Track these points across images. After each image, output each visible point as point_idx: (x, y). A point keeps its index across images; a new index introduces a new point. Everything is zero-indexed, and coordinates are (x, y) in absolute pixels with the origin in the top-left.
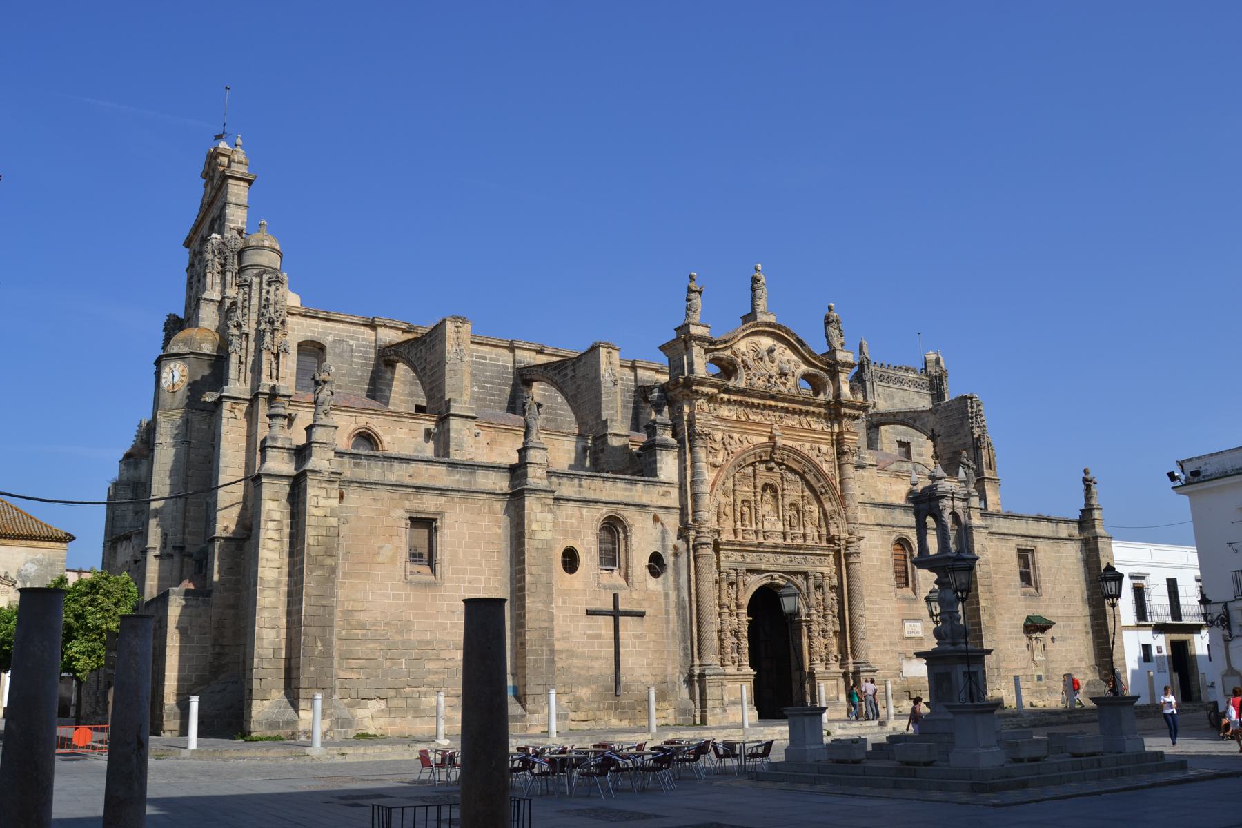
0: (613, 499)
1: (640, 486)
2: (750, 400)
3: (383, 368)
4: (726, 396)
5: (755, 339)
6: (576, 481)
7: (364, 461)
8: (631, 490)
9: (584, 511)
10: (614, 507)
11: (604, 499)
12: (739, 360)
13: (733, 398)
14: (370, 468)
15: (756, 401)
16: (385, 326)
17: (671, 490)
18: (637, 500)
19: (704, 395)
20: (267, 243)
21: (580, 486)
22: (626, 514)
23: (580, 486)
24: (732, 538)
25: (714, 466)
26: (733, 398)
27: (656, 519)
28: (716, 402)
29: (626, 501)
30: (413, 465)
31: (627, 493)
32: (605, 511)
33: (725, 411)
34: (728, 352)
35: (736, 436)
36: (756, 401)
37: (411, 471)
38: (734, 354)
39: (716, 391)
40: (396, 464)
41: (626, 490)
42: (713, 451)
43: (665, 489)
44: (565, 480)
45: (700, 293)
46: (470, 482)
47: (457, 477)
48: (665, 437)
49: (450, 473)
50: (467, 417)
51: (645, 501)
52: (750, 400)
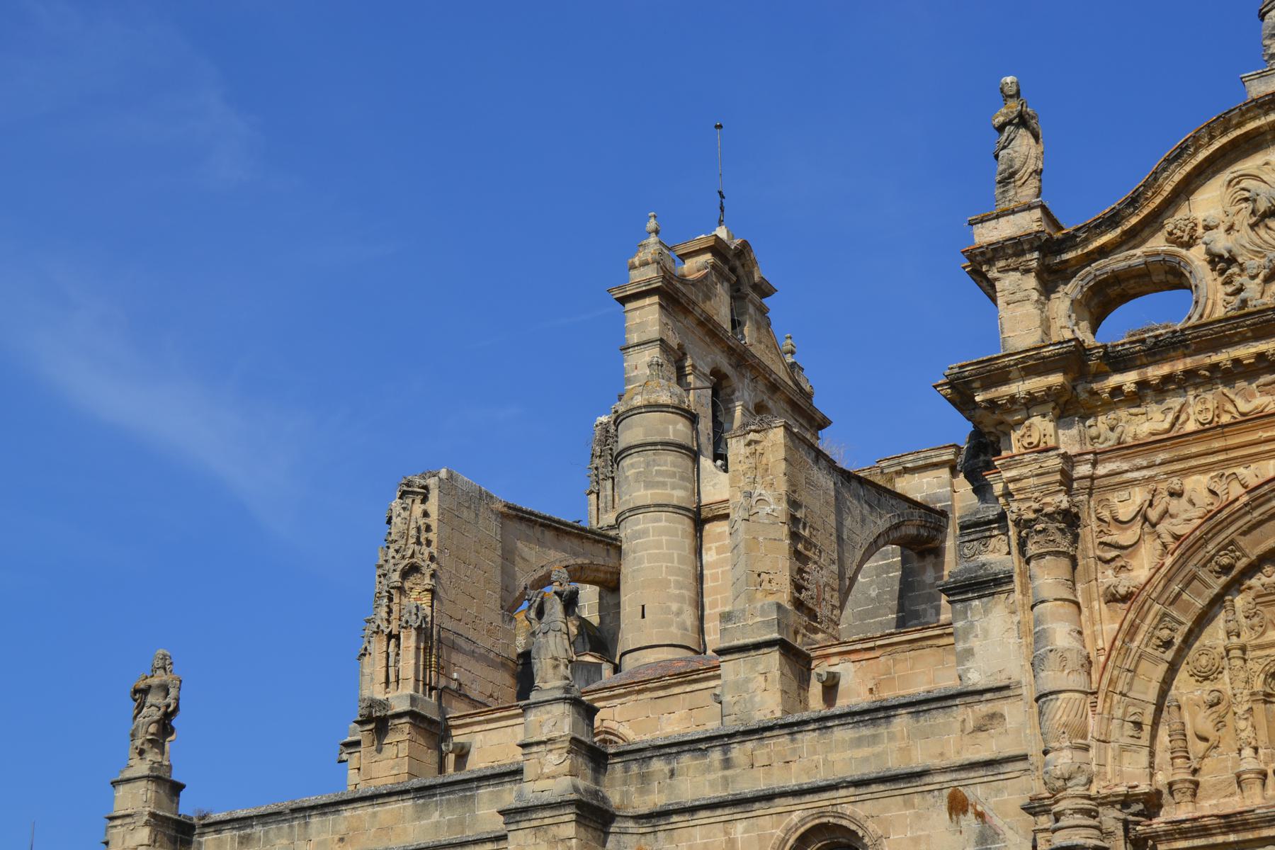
0: (819, 778)
1: (902, 722)
2: (1223, 357)
3: (916, 564)
4: (1128, 379)
5: (1249, 165)
6: (716, 755)
7: (258, 830)
8: (874, 739)
9: (739, 830)
10: (823, 800)
11: (792, 783)
12: (1196, 256)
13: (1155, 373)
14: (267, 841)
15: (1246, 352)
16: (906, 470)
17: (1005, 707)
18: (895, 764)
19: (1032, 402)
20: (638, 401)
21: (727, 763)
22: (860, 811)
23: (727, 763)
24: (1234, 804)
25: (1113, 598)
26: (1155, 373)
27: (958, 805)
28: (1109, 406)
29: (856, 773)
30: (347, 812)
31: (865, 751)
32: (798, 815)
33: (1150, 421)
34: (1158, 243)
35: (1197, 485)
36: (1246, 352)
37: (342, 828)
38: (1172, 239)
39: (1056, 379)
40: (315, 821)
41: (858, 743)
42: (1119, 555)
43: (984, 709)
44: (686, 759)
45: (1022, 121)
46: (461, 822)
47: (436, 816)
48: (983, 558)
49: (420, 813)
50: (757, 646)
51: (918, 761)
52: (1223, 357)
